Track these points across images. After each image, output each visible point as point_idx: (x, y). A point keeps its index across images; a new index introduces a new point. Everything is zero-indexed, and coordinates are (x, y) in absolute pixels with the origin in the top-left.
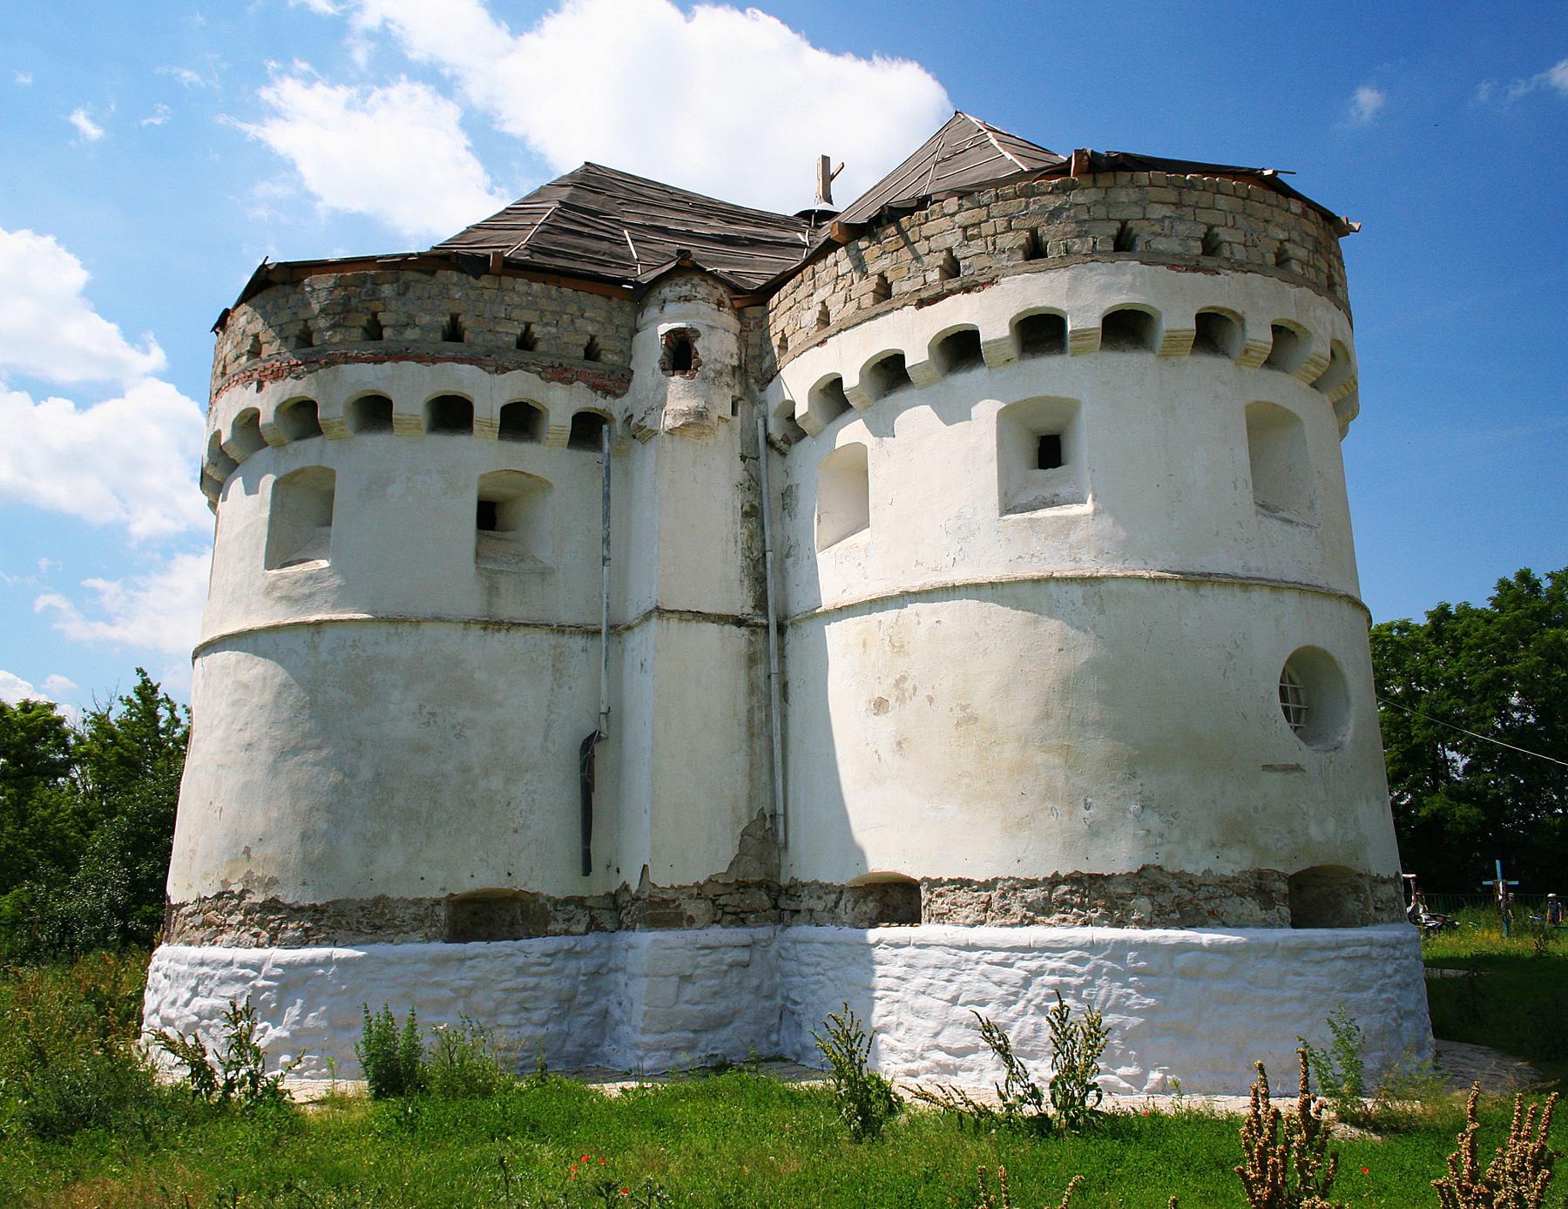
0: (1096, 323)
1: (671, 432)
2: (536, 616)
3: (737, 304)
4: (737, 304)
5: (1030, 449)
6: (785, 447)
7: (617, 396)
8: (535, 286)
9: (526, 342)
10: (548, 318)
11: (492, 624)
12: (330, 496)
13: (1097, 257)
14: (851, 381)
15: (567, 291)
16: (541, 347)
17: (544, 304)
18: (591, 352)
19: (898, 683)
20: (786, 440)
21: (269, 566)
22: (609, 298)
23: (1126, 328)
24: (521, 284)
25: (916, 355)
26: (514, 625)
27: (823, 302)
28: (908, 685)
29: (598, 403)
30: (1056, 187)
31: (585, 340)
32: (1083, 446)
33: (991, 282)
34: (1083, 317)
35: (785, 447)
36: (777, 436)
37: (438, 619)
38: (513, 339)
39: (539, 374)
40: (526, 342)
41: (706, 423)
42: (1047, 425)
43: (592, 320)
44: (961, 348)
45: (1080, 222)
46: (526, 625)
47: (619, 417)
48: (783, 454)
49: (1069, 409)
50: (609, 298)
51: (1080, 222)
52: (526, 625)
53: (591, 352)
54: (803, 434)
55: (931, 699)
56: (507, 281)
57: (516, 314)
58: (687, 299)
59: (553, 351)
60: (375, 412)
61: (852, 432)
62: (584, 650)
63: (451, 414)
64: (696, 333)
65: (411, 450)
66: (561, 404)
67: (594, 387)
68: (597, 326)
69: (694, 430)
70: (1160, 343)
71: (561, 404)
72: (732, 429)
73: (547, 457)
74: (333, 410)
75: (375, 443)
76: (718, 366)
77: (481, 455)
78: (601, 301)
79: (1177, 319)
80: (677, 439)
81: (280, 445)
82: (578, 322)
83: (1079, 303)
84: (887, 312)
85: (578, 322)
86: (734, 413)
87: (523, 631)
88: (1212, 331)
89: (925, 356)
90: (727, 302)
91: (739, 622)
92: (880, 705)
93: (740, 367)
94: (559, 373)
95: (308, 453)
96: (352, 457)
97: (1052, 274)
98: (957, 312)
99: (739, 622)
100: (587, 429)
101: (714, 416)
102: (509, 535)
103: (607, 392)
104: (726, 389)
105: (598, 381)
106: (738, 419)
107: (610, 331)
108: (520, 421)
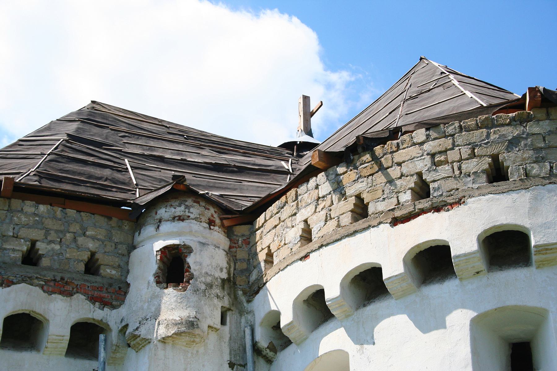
1: (164, 340)
3: (226, 223)
4: (226, 223)
6: (270, 354)
7: (114, 307)
8: (42, 208)
9: (31, 258)
10: (53, 236)
13: (553, 179)
14: (332, 292)
15: (71, 212)
16: (45, 262)
17: (49, 223)
18: (91, 267)
20: (273, 348)
22: (110, 218)
24: (29, 207)
25: (393, 268)
27: (306, 221)
29: (96, 314)
30: (513, 119)
31: (86, 256)
33: (459, 202)
35: (270, 354)
36: (263, 343)
38: (19, 255)
39: (42, 287)
40: (31, 258)
41: (197, 331)
42: (517, 331)
43: (93, 238)
44: (433, 262)
45: (537, 150)
47: (115, 327)
48: (269, 361)
49: (539, 318)
50: (110, 218)
51: (537, 150)
53: (91, 267)
54: (286, 342)
56: (16, 203)
57: (23, 233)
58: (181, 219)
59: (56, 266)
61: (334, 339)
64: (189, 250)
66: (61, 314)
67: (93, 299)
68: (97, 244)
69: (185, 339)
71: (61, 314)
72: (221, 338)
76: (209, 279)
78: (101, 220)
80: (169, 347)
82: (81, 240)
83: (540, 220)
84: (364, 229)
85: (81, 240)
86: (223, 322)
90: (218, 221)
93: (229, 280)
94: (61, 286)
97: (514, 195)
98: (429, 229)
100: (84, 339)
101: (204, 326)
103: (105, 304)
104: (216, 301)
105: (96, 294)
106: (227, 328)
107: (110, 247)
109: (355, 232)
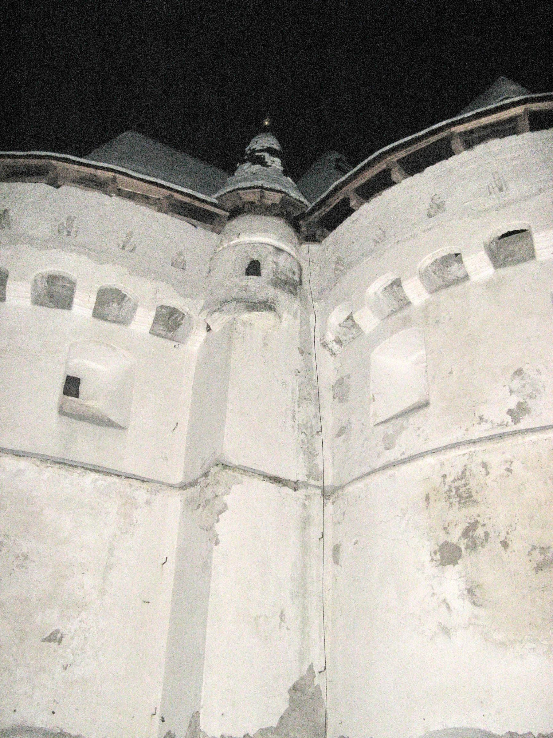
2: (109, 464)
19: (466, 533)
28: (480, 532)
55: (505, 544)
62: (148, 503)
92: (448, 555)
99: (295, 486)
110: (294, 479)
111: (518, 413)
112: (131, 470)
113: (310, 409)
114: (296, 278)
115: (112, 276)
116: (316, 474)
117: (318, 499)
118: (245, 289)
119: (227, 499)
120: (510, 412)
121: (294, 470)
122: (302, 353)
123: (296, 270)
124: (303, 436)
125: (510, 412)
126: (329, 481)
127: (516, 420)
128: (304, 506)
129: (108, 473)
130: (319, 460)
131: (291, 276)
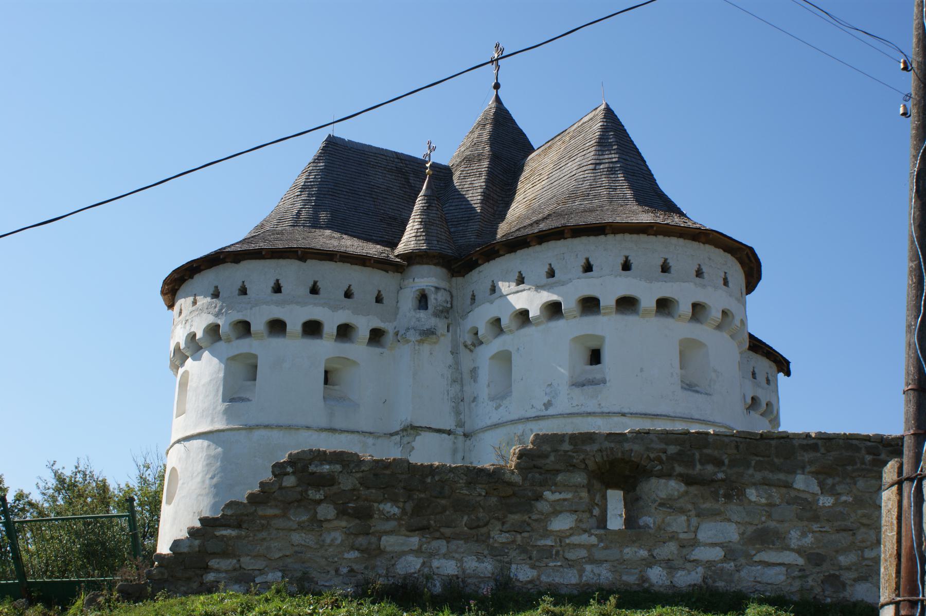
0: (613, 303)
2: (352, 427)
5: (586, 356)
11: (333, 430)
12: (256, 367)
20: (474, 345)
21: (224, 401)
23: (627, 304)
26: (342, 431)
32: (606, 356)
34: (608, 300)
36: (469, 343)
37: (308, 428)
42: (594, 345)
46: (348, 431)
48: (471, 351)
52: (348, 431)
54: (481, 343)
60: (277, 327)
62: (374, 445)
63: (312, 329)
65: (294, 345)
70: (641, 312)
73: (358, 349)
74: (259, 325)
75: (277, 342)
77: (326, 348)
79: (648, 302)
81: (229, 341)
86: (448, 331)
87: (346, 434)
88: (664, 305)
89: (538, 313)
91: (449, 432)
95: (244, 346)
96: (263, 347)
99: (449, 432)
100: (376, 336)
102: (336, 387)
106: (450, 334)
108: (345, 332)
109: (518, 292)
110: (448, 429)
111: (548, 405)
112: (365, 429)
113: (457, 387)
114: (449, 305)
115: (343, 317)
116: (461, 424)
117: (461, 439)
118: (419, 320)
119: (413, 444)
120: (544, 404)
121: (449, 424)
122: (452, 353)
123: (449, 299)
124: (453, 404)
125: (544, 404)
126: (468, 428)
127: (546, 409)
128: (454, 443)
129: (353, 432)
130: (462, 417)
131: (445, 305)
